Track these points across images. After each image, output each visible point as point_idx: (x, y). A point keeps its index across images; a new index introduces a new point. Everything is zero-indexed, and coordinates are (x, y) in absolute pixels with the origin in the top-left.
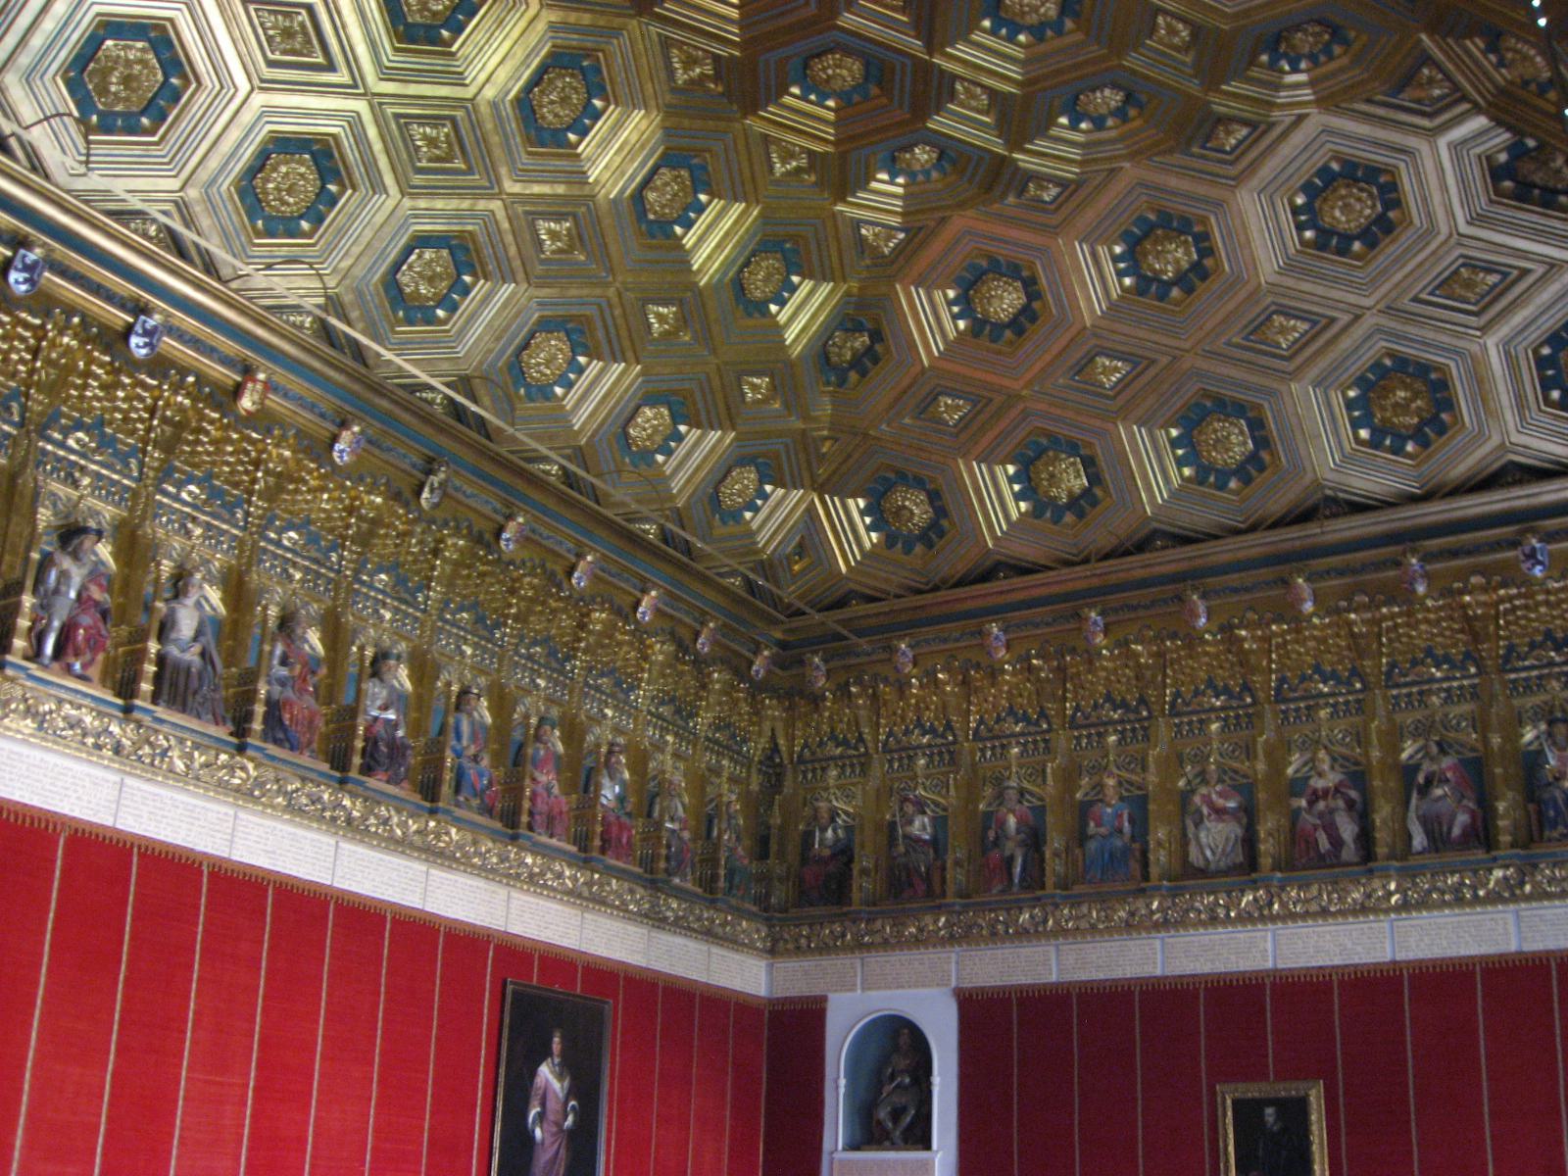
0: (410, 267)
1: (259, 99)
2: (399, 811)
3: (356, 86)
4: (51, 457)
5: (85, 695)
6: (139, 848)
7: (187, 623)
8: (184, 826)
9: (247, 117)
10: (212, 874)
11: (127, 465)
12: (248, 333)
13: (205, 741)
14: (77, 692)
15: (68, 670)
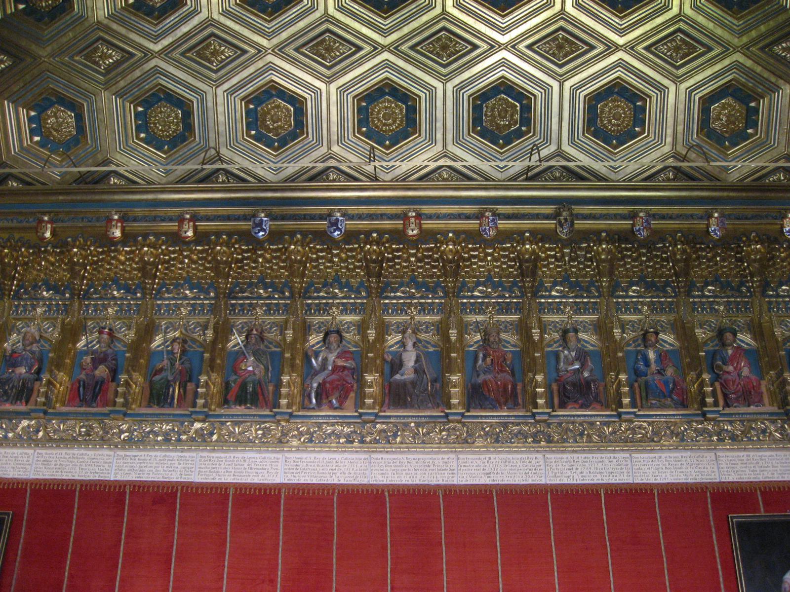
0: (486, 115)
1: (333, 87)
2: (773, 422)
3: (396, 48)
4: (468, 305)
5: (335, 416)
6: (389, 491)
7: (410, 359)
8: (419, 472)
9: (333, 98)
10: (445, 496)
11: (666, 292)
12: (404, 198)
13: (423, 420)
14: (329, 416)
15: (332, 408)
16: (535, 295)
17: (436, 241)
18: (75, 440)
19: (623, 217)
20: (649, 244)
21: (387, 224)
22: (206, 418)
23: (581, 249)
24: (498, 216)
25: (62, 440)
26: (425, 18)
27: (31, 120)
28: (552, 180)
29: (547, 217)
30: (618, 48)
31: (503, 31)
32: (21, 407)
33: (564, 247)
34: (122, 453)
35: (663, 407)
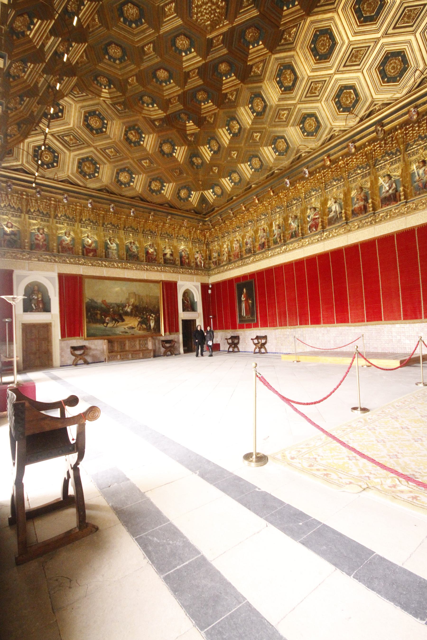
16: (375, 166)
17: (336, 162)
18: (261, 259)
19: (405, 114)
20: (418, 121)
21: (320, 165)
22: (285, 245)
23: (389, 138)
24: (354, 142)
25: (293, 249)
26: (304, 84)
27: (229, 180)
28: (377, 112)
29: (373, 132)
30: (379, 39)
31: (330, 68)
32: (250, 255)
33: (381, 141)
34: (270, 259)
35: (423, 193)
